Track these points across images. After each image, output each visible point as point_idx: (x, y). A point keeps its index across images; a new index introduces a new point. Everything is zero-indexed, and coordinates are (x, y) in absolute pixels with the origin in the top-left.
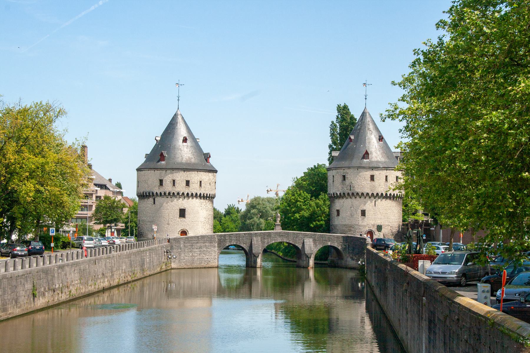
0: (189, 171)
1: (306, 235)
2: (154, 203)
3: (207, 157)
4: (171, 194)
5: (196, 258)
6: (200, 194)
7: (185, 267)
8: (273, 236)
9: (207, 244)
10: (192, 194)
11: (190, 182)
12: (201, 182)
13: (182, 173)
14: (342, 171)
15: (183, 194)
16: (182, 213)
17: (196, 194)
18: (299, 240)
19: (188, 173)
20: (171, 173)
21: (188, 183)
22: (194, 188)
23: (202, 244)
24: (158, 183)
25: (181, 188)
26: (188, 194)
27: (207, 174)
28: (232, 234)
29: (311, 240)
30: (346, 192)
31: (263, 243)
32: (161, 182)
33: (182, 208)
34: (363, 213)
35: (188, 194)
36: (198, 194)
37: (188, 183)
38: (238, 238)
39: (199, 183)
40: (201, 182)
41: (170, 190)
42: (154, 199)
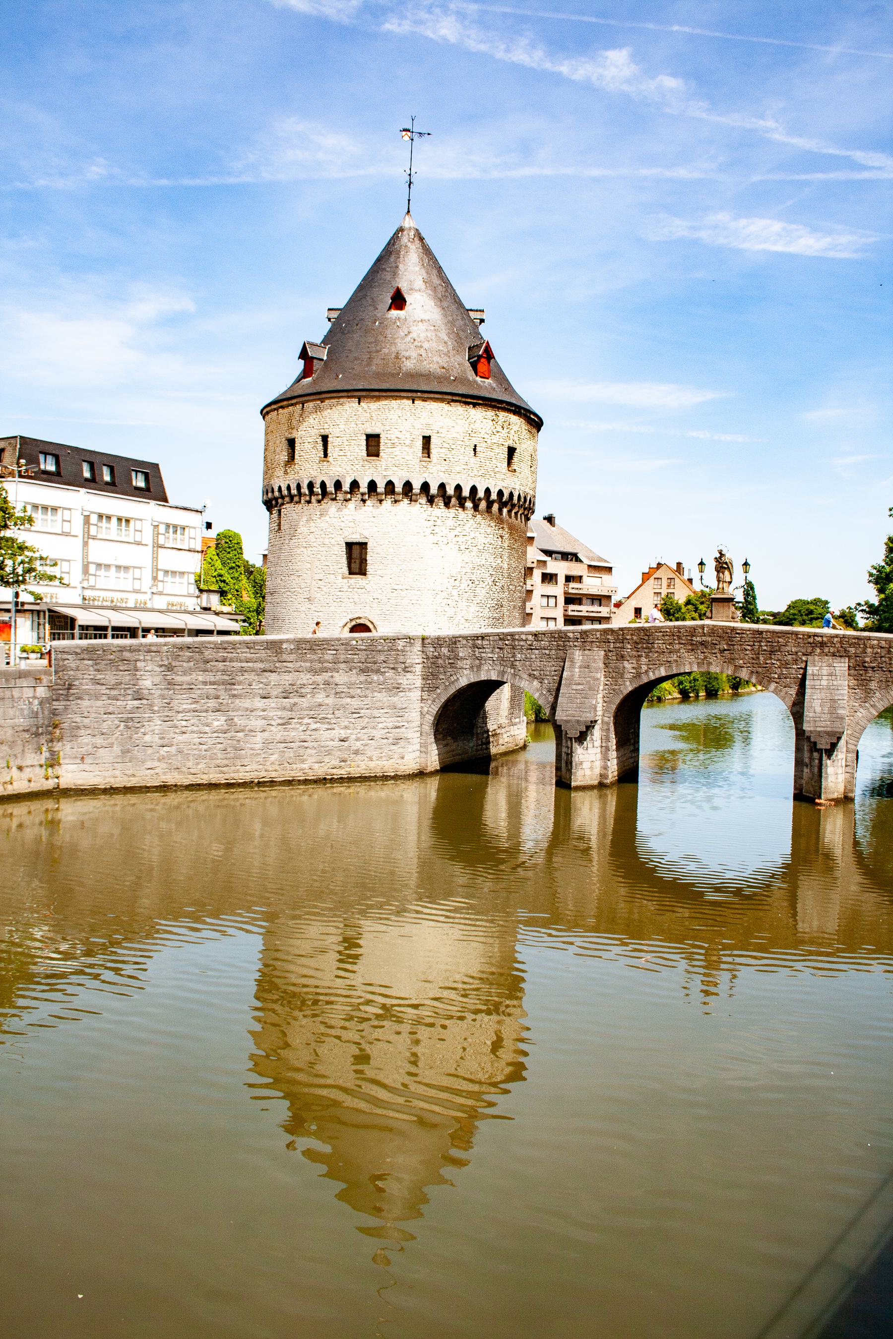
0: (378, 398)
1: (814, 645)
4: (317, 490)
5: (259, 738)
6: (425, 487)
7: (171, 778)
8: (659, 644)
9: (340, 677)
10: (390, 485)
12: (427, 440)
13: (351, 406)
15: (355, 485)
16: (357, 557)
17: (408, 486)
18: (786, 665)
20: (317, 409)
21: (373, 443)
22: (400, 464)
23: (305, 678)
25: (348, 463)
26: (372, 486)
27: (459, 409)
29: (841, 666)
31: (614, 674)
33: (356, 538)
35: (372, 486)
37: (373, 443)
38: (507, 653)
39: (419, 443)
40: (427, 440)
41: (314, 473)
42: (280, 511)
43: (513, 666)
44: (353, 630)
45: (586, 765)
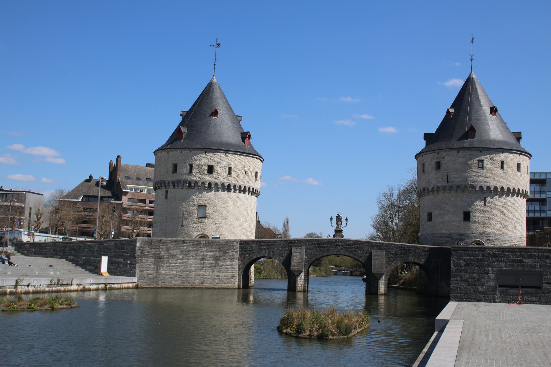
2: (166, 197)
3: (245, 136)
11: (214, 168)
12: (230, 169)
14: (435, 155)
19: (211, 154)
22: (220, 176)
24: (171, 169)
28: (262, 241)
30: (441, 183)
32: (175, 167)
34: (467, 216)
36: (226, 185)
37: (210, 169)
39: (227, 170)
40: (230, 169)
42: (167, 192)
43: (273, 252)
44: (200, 238)
45: (300, 285)
